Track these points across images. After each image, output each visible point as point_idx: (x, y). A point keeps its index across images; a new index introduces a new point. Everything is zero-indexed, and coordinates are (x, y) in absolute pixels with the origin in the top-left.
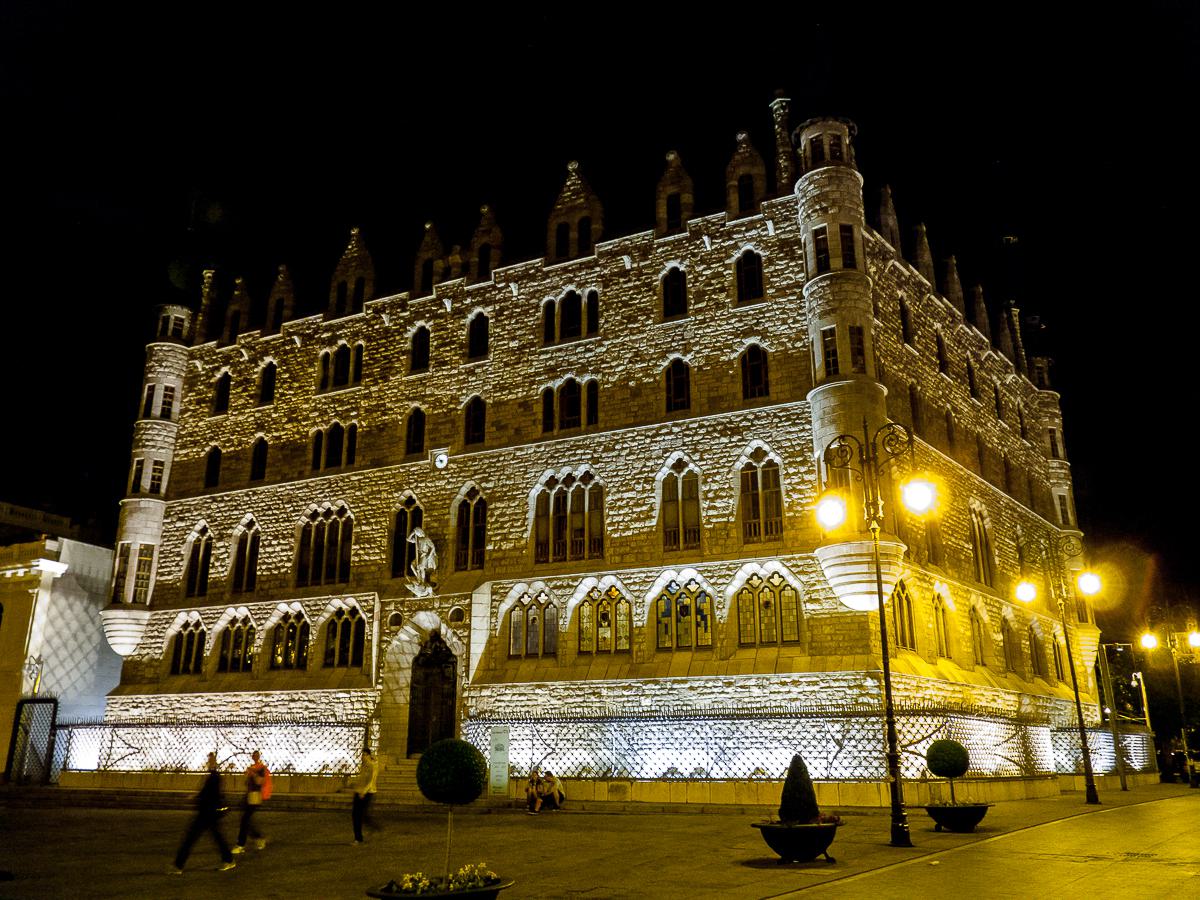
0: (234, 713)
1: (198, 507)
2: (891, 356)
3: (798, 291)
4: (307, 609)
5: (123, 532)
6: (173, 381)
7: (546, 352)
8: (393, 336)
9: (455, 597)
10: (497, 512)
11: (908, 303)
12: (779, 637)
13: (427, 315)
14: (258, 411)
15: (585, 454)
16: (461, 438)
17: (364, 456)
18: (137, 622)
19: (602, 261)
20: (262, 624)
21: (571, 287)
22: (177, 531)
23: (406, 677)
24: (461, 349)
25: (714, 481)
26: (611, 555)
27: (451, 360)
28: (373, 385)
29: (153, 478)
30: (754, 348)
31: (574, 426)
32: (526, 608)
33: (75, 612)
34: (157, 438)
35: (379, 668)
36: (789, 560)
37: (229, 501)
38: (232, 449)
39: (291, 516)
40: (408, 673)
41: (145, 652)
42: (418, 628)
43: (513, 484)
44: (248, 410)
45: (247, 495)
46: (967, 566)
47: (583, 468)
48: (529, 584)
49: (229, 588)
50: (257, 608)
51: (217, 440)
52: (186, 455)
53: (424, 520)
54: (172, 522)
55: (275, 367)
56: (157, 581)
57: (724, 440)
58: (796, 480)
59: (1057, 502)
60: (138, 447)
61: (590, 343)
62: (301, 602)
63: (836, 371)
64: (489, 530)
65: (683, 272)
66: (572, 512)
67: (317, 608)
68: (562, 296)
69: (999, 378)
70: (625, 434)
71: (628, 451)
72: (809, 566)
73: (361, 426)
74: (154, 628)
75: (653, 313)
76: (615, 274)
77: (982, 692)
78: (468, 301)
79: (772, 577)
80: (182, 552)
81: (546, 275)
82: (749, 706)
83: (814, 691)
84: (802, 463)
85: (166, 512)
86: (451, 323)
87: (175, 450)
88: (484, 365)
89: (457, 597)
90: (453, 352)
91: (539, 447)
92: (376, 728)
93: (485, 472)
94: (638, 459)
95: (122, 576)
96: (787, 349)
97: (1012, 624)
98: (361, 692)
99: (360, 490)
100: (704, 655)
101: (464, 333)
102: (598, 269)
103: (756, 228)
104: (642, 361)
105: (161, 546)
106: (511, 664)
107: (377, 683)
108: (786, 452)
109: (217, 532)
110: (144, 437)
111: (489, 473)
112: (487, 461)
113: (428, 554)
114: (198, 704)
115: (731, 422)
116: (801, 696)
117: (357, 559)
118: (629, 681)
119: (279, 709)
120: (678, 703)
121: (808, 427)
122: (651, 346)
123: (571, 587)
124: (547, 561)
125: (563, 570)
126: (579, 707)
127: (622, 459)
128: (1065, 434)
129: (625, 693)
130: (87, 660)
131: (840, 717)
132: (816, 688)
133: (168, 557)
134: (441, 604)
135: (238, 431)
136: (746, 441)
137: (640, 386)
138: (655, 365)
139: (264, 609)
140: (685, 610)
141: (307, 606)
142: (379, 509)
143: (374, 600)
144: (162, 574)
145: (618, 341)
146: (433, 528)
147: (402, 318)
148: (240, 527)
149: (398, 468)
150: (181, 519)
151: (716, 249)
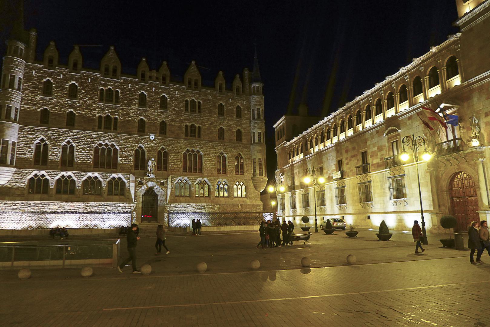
1: (39, 131)
4: (102, 176)
9: (161, 179)
10: (172, 156)
16: (158, 132)
26: (205, 173)
34: (16, 98)
38: (56, 112)
39: (91, 143)
42: (147, 186)
44: (64, 99)
45: (67, 131)
49: (60, 164)
51: (47, 106)
54: (23, 134)
73: (120, 119)
78: (161, 90)
80: (32, 147)
89: (162, 179)
90: (155, 105)
91: (185, 141)
93: (168, 144)
99: (122, 140)
100: (227, 199)
102: (202, 96)
106: (177, 198)
109: (52, 143)
110: (11, 97)
112: (169, 141)
117: (121, 162)
126: (199, 209)
135: (59, 106)
141: (101, 175)
149: (137, 136)
150: (31, 134)
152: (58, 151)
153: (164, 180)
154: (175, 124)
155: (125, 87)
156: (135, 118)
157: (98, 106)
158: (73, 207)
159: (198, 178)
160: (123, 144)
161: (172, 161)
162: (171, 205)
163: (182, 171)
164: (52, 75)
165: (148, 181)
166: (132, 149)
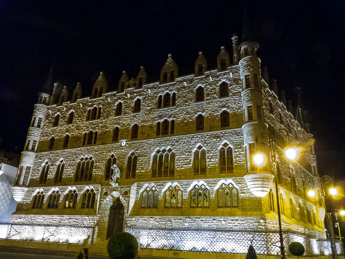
0: (51, 222)
2: (267, 117)
3: (239, 94)
4: (78, 189)
5: (21, 162)
6: (42, 116)
7: (159, 111)
8: (111, 104)
9: (125, 187)
11: (271, 102)
12: (231, 204)
13: (122, 99)
14: (67, 126)
15: (169, 143)
16: (130, 137)
17: (99, 141)
18: (23, 191)
19: (177, 84)
20: (63, 193)
21: (167, 91)
22: (39, 162)
23: (108, 213)
24: (132, 109)
25: (211, 153)
27: (129, 112)
28: (103, 119)
29: (33, 146)
30: (225, 112)
31: (166, 134)
32: (148, 192)
33: (4, 187)
34: (35, 133)
35: (99, 209)
36: (235, 179)
37: (56, 154)
38: (58, 137)
39: (75, 159)
40: (108, 211)
41: (25, 201)
42: (113, 197)
43: (146, 152)
45: (62, 152)
46: (289, 185)
47: (169, 147)
48: (149, 184)
50: (61, 188)
52: (44, 139)
53: (117, 162)
54: (37, 160)
55: (74, 113)
56: (31, 178)
57: (215, 140)
58: (238, 153)
59: (312, 168)
60: (29, 136)
61: (173, 108)
62: (75, 187)
63: (252, 119)
64: (137, 166)
65: (203, 88)
66: (164, 161)
67: (81, 189)
68: (164, 94)
69: (296, 128)
70: (183, 137)
71: (183, 142)
72: (242, 181)
73: (99, 132)
74: (28, 193)
75: (193, 100)
76: (182, 88)
77: (294, 226)
78: (135, 94)
79: (229, 185)
80: (40, 169)
81: (160, 87)
82: (222, 227)
83: (243, 223)
84: (240, 148)
85: (36, 156)
86: (129, 101)
87: (40, 137)
88: (139, 114)
91: (155, 140)
92: (97, 229)
93: (137, 148)
94: (187, 145)
95: (19, 176)
96: (236, 112)
97: (301, 205)
98: (93, 217)
99: (97, 151)
100: (206, 210)
101: (133, 104)
102: (176, 86)
103: (226, 75)
104: (189, 115)
105: (33, 167)
106: (142, 210)
107: (98, 214)
108: (235, 144)
109: (51, 163)
110: (31, 133)
111: (139, 148)
112: (138, 144)
113: (118, 172)
114: (40, 218)
115: (217, 134)
116: (238, 225)
117: (94, 174)
118: (181, 217)
119: (66, 221)
120: (197, 225)
121: (242, 136)
122: (192, 110)
123: (163, 185)
124: (156, 177)
125: (160, 180)
126: (164, 225)
127: (181, 145)
128: (315, 147)
129: (180, 221)
130: (7, 203)
131: (253, 232)
132: (244, 222)
133: (35, 171)
134: (120, 189)
135: (60, 132)
136: (222, 140)
137: (188, 122)
138: (193, 116)
139: (64, 188)
140: (200, 194)
142: (103, 158)
143: (99, 187)
144: (33, 176)
145: (182, 108)
146: (120, 164)
147: (114, 99)
148: (59, 162)
150: (40, 159)
151: (214, 81)
152: (54, 170)
153: (127, 189)
154: (146, 124)
155: (106, 102)
156: (111, 128)
157: (84, 125)
158: (52, 220)
159: (167, 182)
160: (97, 156)
161: (139, 166)
162: (132, 218)
163: (151, 176)
164: (60, 110)
165: (112, 191)
166: (105, 158)
